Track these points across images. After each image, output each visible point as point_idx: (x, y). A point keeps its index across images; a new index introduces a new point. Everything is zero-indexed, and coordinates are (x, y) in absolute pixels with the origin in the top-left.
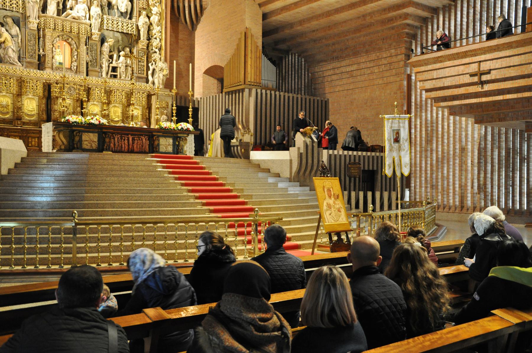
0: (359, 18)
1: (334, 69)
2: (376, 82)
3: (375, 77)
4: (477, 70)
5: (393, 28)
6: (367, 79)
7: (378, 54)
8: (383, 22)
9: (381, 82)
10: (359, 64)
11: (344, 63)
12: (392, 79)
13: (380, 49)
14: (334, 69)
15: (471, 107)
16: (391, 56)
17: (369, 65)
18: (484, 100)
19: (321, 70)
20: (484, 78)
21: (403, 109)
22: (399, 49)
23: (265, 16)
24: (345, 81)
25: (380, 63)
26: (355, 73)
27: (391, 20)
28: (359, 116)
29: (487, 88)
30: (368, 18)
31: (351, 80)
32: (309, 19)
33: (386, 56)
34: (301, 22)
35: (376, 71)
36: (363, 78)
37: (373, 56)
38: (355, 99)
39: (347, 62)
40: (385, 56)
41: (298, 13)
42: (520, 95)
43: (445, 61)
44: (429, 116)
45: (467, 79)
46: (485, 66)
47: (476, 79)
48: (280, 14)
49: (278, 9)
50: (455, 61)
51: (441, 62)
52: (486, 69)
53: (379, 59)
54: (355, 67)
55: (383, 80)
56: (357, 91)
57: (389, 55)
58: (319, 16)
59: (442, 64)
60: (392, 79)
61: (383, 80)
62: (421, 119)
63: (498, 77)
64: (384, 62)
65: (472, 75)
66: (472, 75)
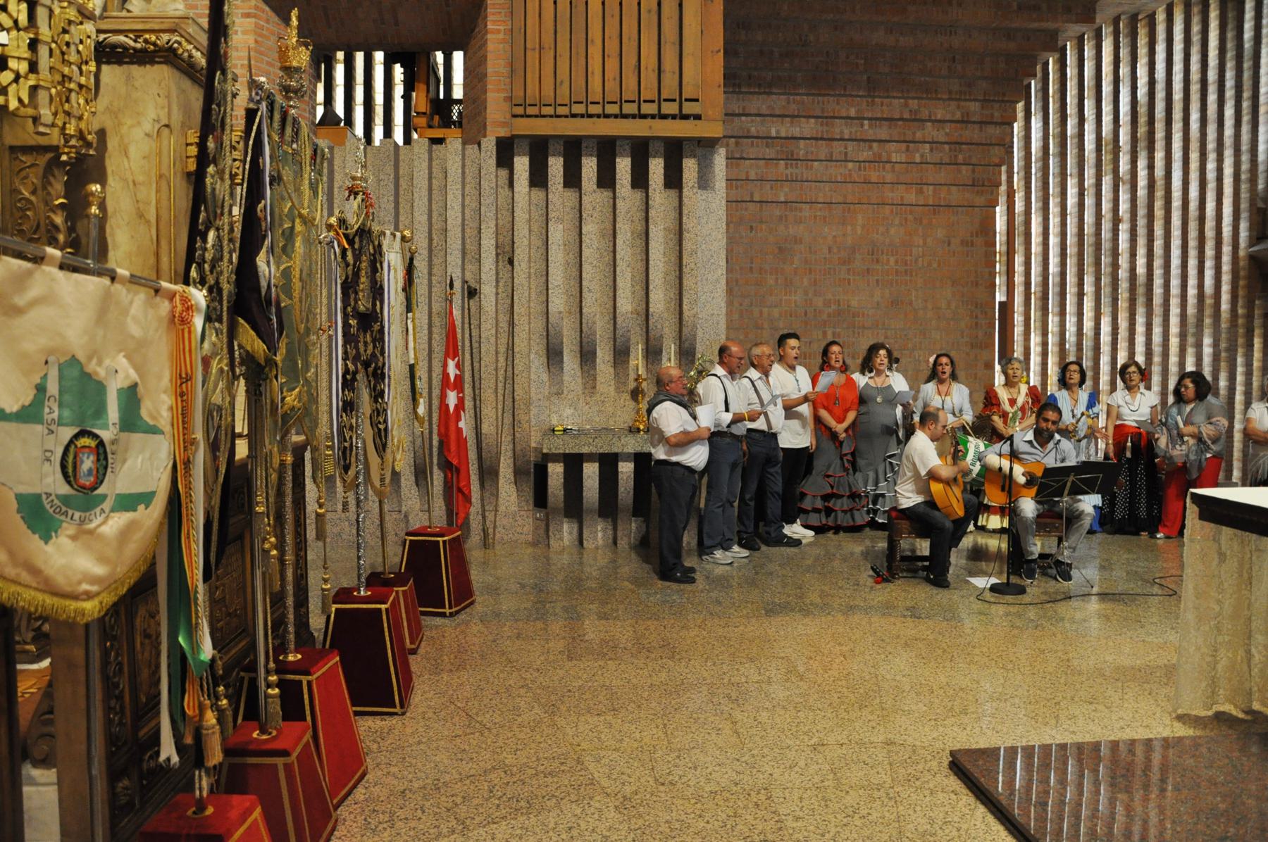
3: (889, 177)
6: (855, 177)
7: (914, 104)
9: (911, 197)
10: (827, 118)
12: (955, 195)
13: (929, 92)
17: (867, 130)
22: (997, 106)
25: (919, 135)
26: (802, 148)
28: (819, 302)
36: (836, 171)
37: (895, 106)
38: (797, 240)
39: (778, 102)
44: (1071, 328)
54: (808, 127)
55: (921, 192)
56: (806, 211)
57: (958, 116)
61: (921, 192)
62: (1045, 334)
64: (930, 131)
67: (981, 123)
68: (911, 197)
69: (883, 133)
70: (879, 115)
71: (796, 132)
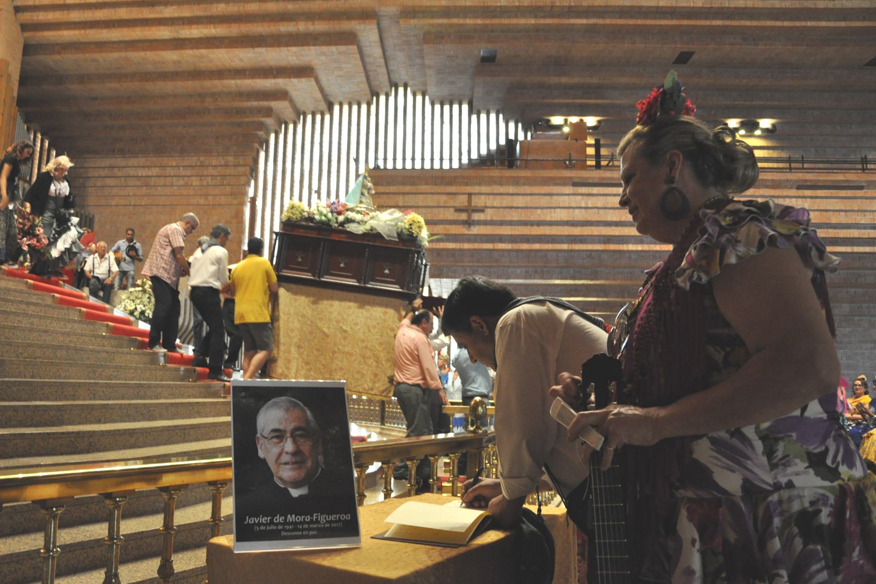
0: (190, 96)
1: (111, 167)
2: (194, 201)
3: (192, 193)
4: (466, 204)
5: (239, 125)
7: (202, 159)
8: (227, 112)
9: (202, 201)
10: (162, 167)
11: (133, 162)
12: (223, 200)
13: (208, 152)
14: (111, 167)
15: (438, 255)
16: (226, 165)
17: (182, 172)
18: (466, 246)
19: (86, 165)
20: (476, 216)
21: (240, 247)
23: (28, 49)
24: (131, 191)
25: (205, 173)
26: (152, 181)
27: (241, 112)
29: (475, 230)
30: (208, 100)
31: (144, 190)
32: (103, 77)
33: (218, 164)
34: (83, 78)
35: (194, 183)
37: (193, 160)
39: (142, 161)
40: (214, 162)
41: (95, 60)
42: (516, 246)
43: (421, 185)
45: (450, 215)
46: (478, 201)
47: (464, 216)
48: (59, 53)
49: (58, 44)
50: (435, 187)
51: (413, 184)
52: (479, 205)
53: (202, 166)
54: (155, 171)
57: (223, 163)
58: (125, 76)
59: (414, 187)
60: (223, 200)
63: (495, 218)
64: (211, 171)
65: (458, 210)
66: (458, 210)
67: (234, 166)
68: (202, 201)
69: (188, 172)
70: (186, 164)
71: (150, 174)
